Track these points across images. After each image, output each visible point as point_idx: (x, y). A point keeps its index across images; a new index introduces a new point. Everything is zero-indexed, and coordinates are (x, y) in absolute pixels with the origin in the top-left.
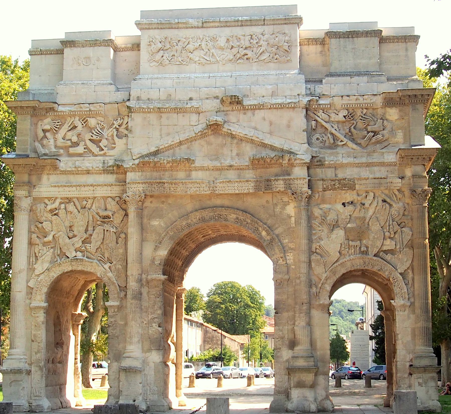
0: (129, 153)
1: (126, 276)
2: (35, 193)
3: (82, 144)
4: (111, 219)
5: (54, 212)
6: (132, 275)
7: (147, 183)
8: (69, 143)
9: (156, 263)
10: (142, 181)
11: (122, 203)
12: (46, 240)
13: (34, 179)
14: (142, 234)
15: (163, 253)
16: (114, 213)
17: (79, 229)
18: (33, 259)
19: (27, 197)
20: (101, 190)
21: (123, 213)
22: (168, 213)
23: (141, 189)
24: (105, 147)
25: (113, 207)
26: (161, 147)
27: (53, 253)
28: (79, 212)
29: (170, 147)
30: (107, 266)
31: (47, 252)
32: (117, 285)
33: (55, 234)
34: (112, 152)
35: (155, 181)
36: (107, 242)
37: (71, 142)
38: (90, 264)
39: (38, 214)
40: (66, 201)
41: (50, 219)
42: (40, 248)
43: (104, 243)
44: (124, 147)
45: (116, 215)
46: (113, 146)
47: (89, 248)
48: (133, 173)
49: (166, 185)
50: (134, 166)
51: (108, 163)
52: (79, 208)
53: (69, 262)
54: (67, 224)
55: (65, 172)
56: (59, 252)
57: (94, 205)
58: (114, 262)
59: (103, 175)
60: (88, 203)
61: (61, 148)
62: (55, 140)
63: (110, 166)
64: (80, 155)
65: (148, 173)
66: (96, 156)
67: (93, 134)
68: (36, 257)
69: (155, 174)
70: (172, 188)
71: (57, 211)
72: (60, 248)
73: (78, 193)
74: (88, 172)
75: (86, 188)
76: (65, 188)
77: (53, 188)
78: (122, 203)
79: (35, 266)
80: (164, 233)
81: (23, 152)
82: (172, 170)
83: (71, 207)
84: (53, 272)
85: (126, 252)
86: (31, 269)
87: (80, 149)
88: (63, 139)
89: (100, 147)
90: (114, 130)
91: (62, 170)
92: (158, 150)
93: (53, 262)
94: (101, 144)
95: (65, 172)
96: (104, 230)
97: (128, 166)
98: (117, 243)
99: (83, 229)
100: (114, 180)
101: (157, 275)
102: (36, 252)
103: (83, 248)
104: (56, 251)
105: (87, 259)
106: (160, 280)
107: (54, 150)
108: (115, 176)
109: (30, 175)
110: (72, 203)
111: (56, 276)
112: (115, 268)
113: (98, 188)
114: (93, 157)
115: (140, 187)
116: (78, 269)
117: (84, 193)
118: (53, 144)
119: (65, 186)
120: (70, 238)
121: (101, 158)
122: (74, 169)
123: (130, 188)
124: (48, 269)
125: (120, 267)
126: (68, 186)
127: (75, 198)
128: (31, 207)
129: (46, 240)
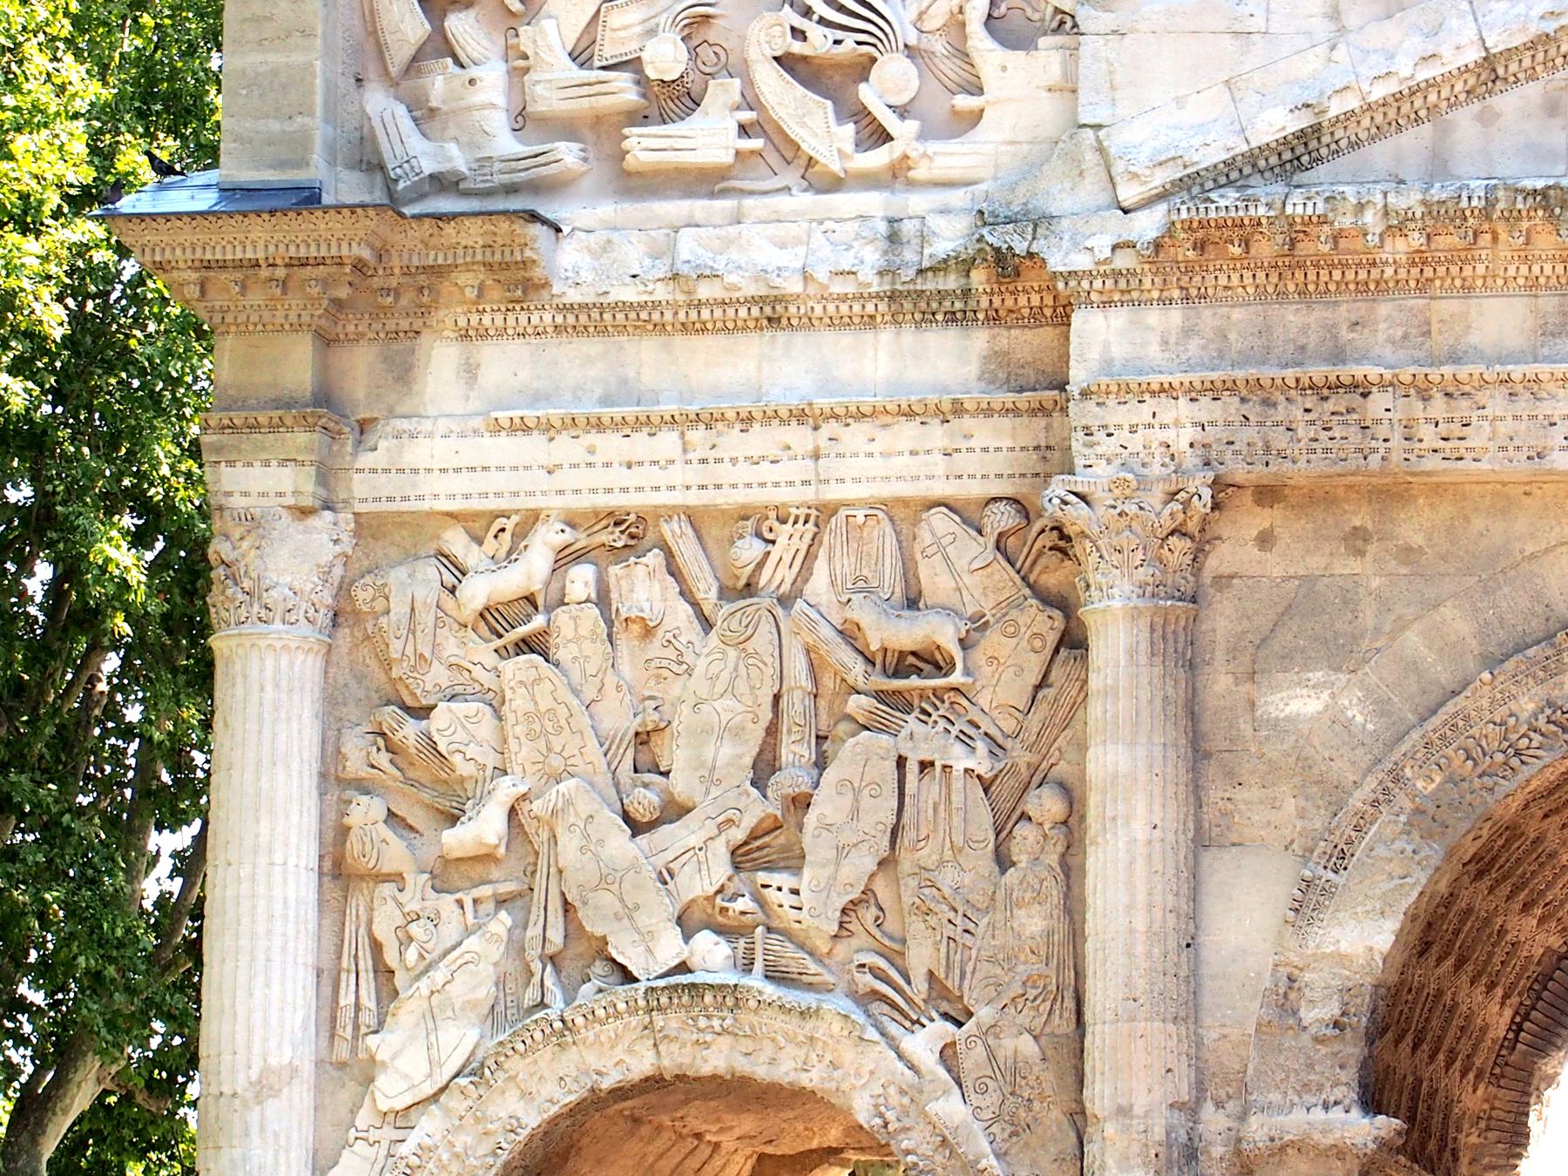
0: (1091, 158)
1: (1078, 1117)
2: (371, 480)
3: (722, 94)
4: (957, 678)
5: (519, 630)
6: (1124, 1112)
7: (1231, 387)
8: (623, 89)
9: (1308, 1015)
10: (1195, 377)
11: (1038, 547)
12: (457, 839)
13: (360, 367)
14: (1196, 790)
15: (1363, 937)
16: (980, 624)
17: (708, 762)
18: (361, 991)
19: (304, 512)
20: (874, 448)
21: (1048, 625)
22: (1401, 626)
23: (1182, 439)
24: (902, 112)
25: (967, 579)
26: (1335, 108)
27: (516, 947)
28: (707, 624)
29: (1408, 108)
30: (923, 1044)
31: (468, 932)
33: (524, 797)
34: (949, 157)
35: (1290, 374)
36: (928, 854)
37: (642, 82)
38: (792, 1024)
39: (396, 647)
40: (604, 538)
41: (487, 679)
42: (414, 906)
43: (906, 864)
44: (1045, 113)
45: (993, 641)
46: (964, 102)
47: (787, 899)
48: (1119, 318)
49: (1378, 403)
50: (1124, 261)
51: (923, 239)
52: (707, 592)
53: (633, 1010)
54: (619, 718)
55: (594, 320)
56: (556, 936)
57: (821, 568)
58: (984, 1014)
59: (886, 335)
60: (776, 551)
61: (567, 128)
62: (519, 67)
63: (940, 267)
64: (706, 182)
65: (1237, 314)
66: (834, 184)
67: (807, 12)
68: (384, 973)
69: (1293, 319)
70: (1427, 433)
71: (538, 621)
72: (567, 907)
73: (693, 475)
74: (772, 313)
75: (761, 439)
76: (593, 438)
77: (503, 439)
78: (1038, 547)
79: (372, 1041)
80: (1371, 783)
81: (281, 165)
82: (1423, 286)
83: (643, 588)
84: (513, 1095)
85: (1076, 935)
86: (346, 1069)
87: (708, 137)
88: (573, 56)
89: (860, 115)
91: (573, 296)
92: (1317, 129)
93: (511, 1012)
94: (867, 94)
95: (594, 320)
96: (901, 762)
97: (1082, 262)
98: (1003, 861)
99: (737, 755)
100: (973, 369)
101: (1318, 1114)
102: (383, 931)
103: (744, 904)
104: (534, 931)
105: (771, 991)
106: (1339, 1152)
107: (506, 144)
108: (980, 340)
109: (326, 341)
110: (655, 558)
111: (532, 1119)
112: (991, 1056)
113: (855, 436)
114: (809, 198)
115: (1180, 426)
116: (706, 1070)
117: (744, 473)
118: (501, 100)
119: (598, 425)
120: (637, 828)
121: (874, 203)
122: (661, 293)
123: (1100, 436)
124: (474, 1070)
125: (1027, 1046)
126: (619, 424)
127: (670, 512)
128: (344, 589)
129: (457, 839)
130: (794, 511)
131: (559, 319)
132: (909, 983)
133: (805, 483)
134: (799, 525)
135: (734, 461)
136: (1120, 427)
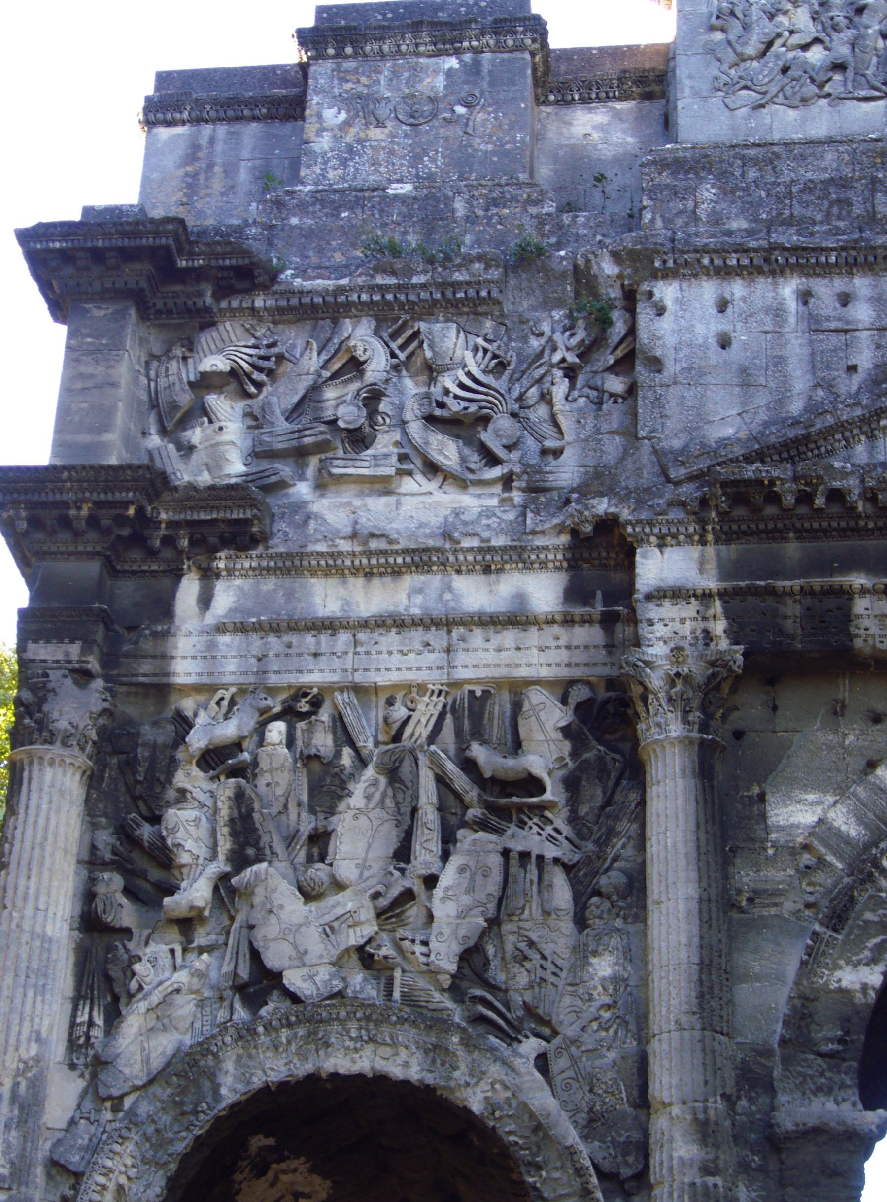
20: (491, 646)
32: (588, 1163)
47: (419, 949)
58: (570, 1031)
76: (293, 639)
90: (558, 374)
94: (486, 437)
113: (477, 636)
116: (355, 1069)
122: (345, 546)
130: (431, 687)
131: (272, 564)
132: (509, 1010)
133: (440, 668)
134: (434, 698)
135: (390, 653)
136: (673, 620)
